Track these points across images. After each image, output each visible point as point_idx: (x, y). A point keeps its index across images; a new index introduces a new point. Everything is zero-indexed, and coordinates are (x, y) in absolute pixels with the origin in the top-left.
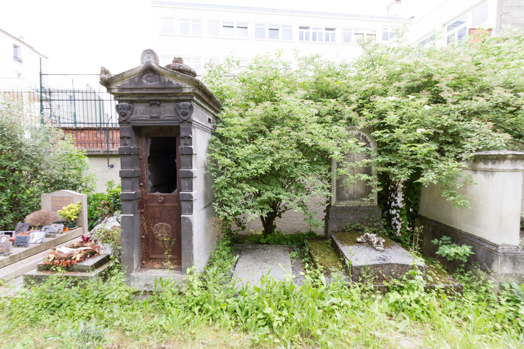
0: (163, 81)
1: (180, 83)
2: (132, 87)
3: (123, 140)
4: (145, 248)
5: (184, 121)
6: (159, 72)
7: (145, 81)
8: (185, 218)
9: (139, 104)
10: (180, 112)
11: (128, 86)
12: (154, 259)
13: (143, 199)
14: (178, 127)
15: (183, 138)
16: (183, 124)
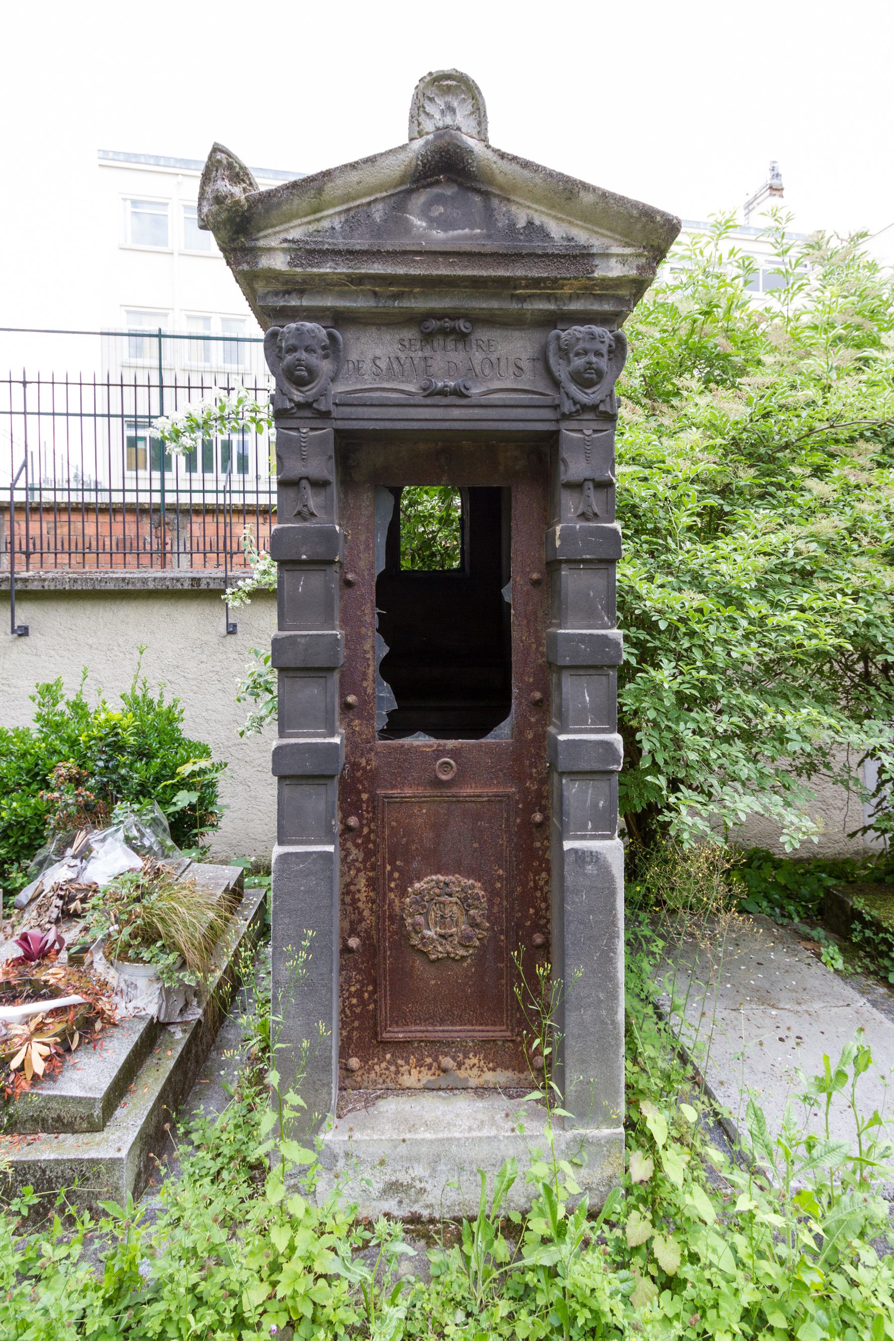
0: (502, 223)
1: (582, 236)
2: (360, 243)
3: (291, 493)
4: (359, 994)
5: (585, 408)
6: (491, 181)
7: (418, 223)
8: (581, 856)
9: (373, 332)
10: (562, 371)
11: (341, 243)
12: (402, 1047)
13: (355, 766)
14: (552, 438)
15: (577, 486)
16: (573, 425)
